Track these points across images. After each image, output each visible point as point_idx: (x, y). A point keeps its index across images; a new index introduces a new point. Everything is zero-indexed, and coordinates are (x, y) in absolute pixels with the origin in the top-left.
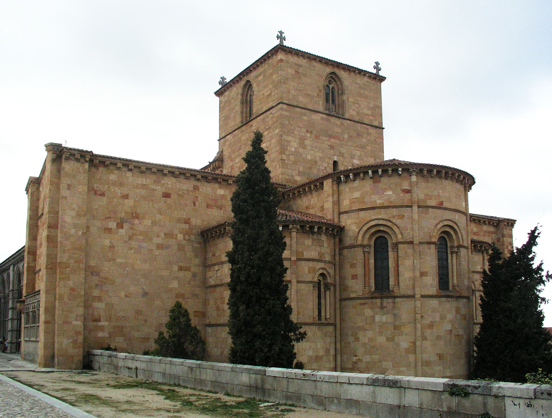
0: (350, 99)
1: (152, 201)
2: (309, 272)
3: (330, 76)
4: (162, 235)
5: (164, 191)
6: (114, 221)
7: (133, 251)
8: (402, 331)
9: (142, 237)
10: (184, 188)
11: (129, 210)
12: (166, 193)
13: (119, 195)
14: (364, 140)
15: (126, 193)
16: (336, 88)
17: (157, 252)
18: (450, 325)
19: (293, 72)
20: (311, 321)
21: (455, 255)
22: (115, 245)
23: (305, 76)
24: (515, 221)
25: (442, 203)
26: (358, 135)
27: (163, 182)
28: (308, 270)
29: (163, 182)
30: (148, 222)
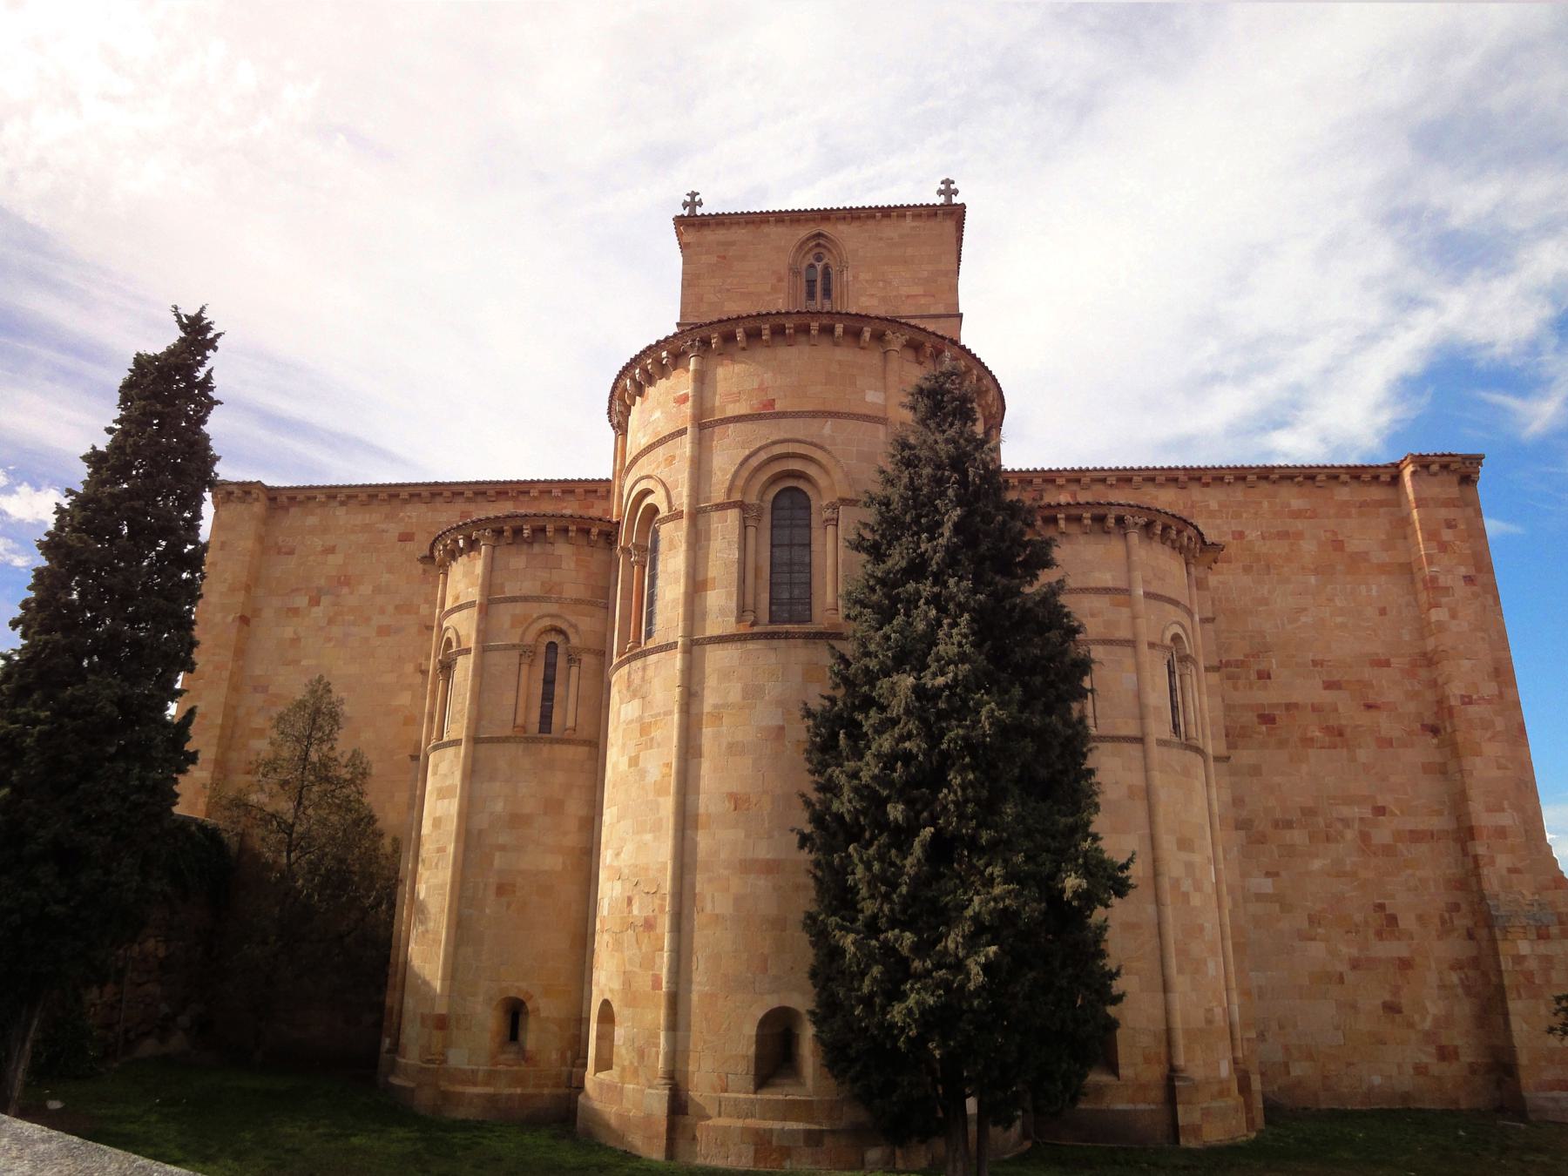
0: (862, 276)
2: (513, 626)
3: (814, 243)
4: (390, 609)
7: (332, 644)
8: (652, 739)
12: (408, 534)
16: (831, 263)
19: (714, 259)
20: (508, 732)
21: (830, 529)
24: (1477, 460)
25: (772, 403)
27: (402, 514)
29: (402, 514)
30: (366, 589)
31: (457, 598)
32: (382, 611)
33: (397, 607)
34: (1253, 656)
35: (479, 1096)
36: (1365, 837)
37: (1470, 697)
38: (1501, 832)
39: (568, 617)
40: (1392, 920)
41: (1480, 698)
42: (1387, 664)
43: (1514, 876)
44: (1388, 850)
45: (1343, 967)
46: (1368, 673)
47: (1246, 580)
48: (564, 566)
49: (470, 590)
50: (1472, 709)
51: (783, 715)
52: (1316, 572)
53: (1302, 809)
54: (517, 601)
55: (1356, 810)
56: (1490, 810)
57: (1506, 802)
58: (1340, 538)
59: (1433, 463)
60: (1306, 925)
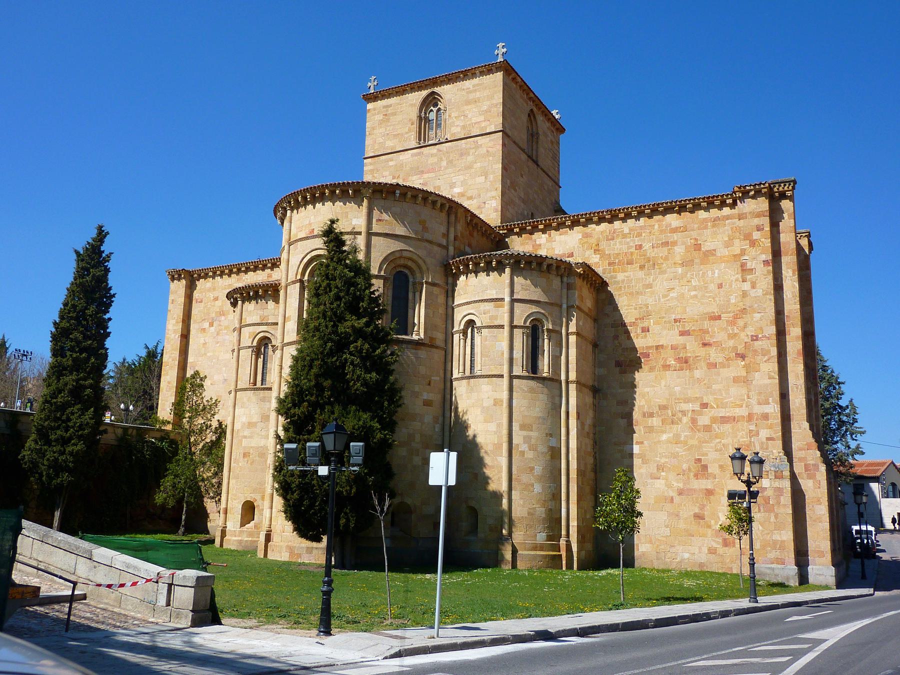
0: (453, 115)
7: (218, 345)
11: (218, 310)
13: (212, 298)
14: (470, 158)
23: (394, 114)
26: (462, 155)
27: (244, 278)
29: (244, 278)
34: (640, 319)
35: (234, 541)
36: (694, 421)
39: (270, 331)
40: (705, 467)
42: (719, 318)
44: (707, 428)
45: (674, 494)
46: (706, 324)
47: (641, 274)
50: (756, 343)
52: (682, 265)
53: (659, 406)
55: (691, 405)
57: (771, 399)
59: (751, 190)
60: (655, 471)
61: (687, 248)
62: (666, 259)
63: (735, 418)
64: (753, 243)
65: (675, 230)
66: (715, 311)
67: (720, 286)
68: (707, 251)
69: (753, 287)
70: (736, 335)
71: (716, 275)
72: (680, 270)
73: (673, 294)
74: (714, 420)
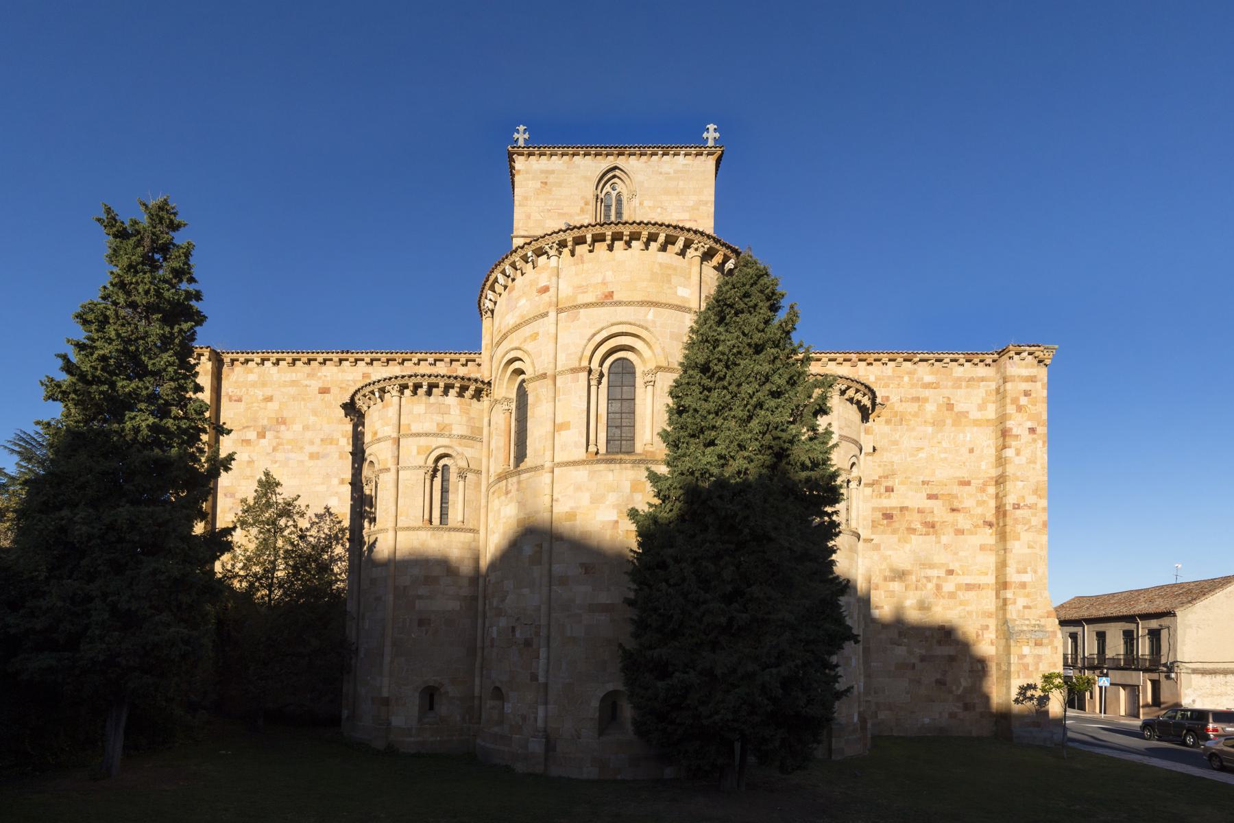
1: (304, 399)
2: (418, 453)
5: (321, 385)
6: (254, 430)
7: (277, 465)
9: (290, 447)
10: (349, 379)
11: (273, 415)
13: (261, 397)
15: (270, 394)
17: (311, 463)
18: (615, 512)
20: (420, 524)
22: (255, 458)
27: (319, 374)
28: (417, 450)
29: (319, 374)
30: (297, 427)
31: (375, 434)
32: (312, 443)
33: (322, 440)
37: (1019, 505)
38: (1023, 585)
41: (1025, 505)
42: (968, 483)
43: (1026, 611)
48: (452, 412)
49: (385, 428)
51: (618, 513)
52: (933, 424)
54: (420, 436)
56: (1018, 572)
58: (952, 402)
61: (939, 406)
62: (916, 415)
63: (980, 585)
64: (1020, 409)
65: (927, 386)
66: (966, 476)
67: (971, 451)
68: (960, 412)
69: (1018, 454)
70: (984, 502)
71: (968, 439)
72: (930, 429)
73: (922, 455)
74: (959, 587)
